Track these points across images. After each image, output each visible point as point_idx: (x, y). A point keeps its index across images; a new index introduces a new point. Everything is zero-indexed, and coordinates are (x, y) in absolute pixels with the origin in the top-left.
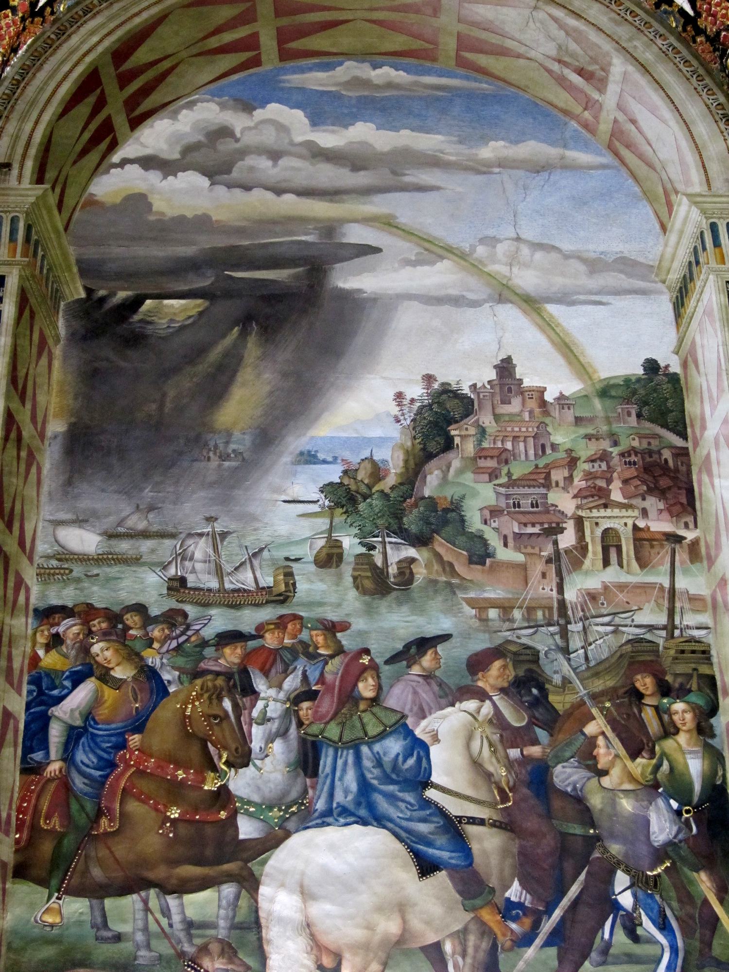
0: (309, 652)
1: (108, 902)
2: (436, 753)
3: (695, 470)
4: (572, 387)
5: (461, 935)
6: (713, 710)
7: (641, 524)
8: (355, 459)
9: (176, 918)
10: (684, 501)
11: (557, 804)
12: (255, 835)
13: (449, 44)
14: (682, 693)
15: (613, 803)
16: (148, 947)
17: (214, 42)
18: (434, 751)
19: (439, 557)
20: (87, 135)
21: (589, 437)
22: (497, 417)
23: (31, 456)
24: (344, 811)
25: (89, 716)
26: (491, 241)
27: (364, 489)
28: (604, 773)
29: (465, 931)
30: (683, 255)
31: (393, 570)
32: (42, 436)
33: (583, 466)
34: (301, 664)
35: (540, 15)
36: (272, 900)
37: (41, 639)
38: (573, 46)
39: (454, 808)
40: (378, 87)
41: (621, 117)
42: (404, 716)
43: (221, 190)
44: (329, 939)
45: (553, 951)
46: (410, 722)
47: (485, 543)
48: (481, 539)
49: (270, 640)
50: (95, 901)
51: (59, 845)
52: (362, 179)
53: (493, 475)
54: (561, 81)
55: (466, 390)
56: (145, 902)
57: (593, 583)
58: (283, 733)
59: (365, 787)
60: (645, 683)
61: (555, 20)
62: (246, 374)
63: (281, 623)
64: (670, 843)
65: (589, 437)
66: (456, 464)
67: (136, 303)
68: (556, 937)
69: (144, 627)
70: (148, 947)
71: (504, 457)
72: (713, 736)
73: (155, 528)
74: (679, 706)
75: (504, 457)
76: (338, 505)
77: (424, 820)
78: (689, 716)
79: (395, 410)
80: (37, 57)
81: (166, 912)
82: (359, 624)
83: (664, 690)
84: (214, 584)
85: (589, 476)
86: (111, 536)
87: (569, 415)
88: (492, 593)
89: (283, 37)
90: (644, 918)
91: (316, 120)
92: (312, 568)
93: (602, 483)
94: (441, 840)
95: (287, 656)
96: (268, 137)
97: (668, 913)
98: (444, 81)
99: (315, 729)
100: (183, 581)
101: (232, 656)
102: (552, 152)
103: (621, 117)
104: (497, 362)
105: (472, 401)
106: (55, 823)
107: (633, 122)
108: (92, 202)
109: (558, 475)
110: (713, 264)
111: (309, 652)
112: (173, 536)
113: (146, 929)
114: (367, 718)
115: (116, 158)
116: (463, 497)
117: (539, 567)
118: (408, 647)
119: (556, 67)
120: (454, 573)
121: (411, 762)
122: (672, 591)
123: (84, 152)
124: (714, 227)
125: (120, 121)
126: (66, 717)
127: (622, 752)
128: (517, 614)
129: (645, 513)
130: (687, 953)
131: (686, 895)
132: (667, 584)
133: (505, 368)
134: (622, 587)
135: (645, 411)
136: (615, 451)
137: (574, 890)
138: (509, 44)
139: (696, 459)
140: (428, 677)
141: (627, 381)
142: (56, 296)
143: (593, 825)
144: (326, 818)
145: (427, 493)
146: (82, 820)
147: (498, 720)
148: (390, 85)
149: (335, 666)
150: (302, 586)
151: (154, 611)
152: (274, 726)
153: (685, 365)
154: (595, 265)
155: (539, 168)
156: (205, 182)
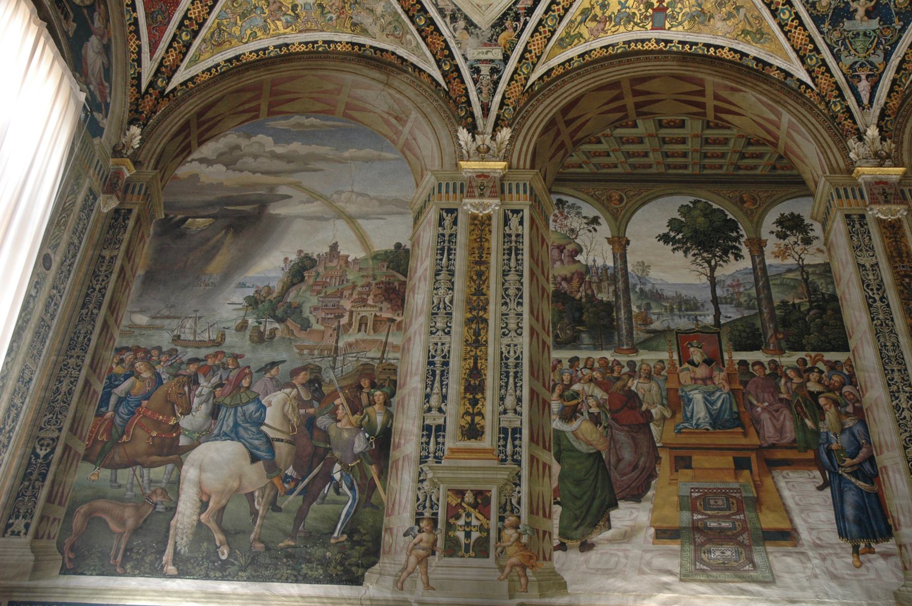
0: (224, 367)
1: (119, 471)
2: (269, 411)
3: (407, 291)
4: (361, 255)
5: (263, 489)
6: (393, 394)
7: (378, 314)
8: (261, 285)
9: (146, 478)
10: (399, 304)
11: (316, 433)
12: (186, 444)
13: (341, 108)
14: (381, 387)
15: (341, 434)
16: (132, 490)
17: (241, 108)
18: (268, 409)
19: (288, 327)
20: (179, 149)
21: (363, 276)
22: (326, 268)
23: (128, 284)
24: (226, 434)
25: (128, 393)
26: (339, 193)
27: (262, 299)
28: (339, 421)
29: (265, 487)
30: (424, 197)
31: (267, 333)
32: (134, 276)
33: (359, 289)
34: (220, 372)
35: (385, 93)
36: (187, 472)
37: (115, 361)
38: (396, 106)
39: (272, 434)
40: (307, 127)
41: (410, 138)
42: (259, 395)
43: (230, 172)
44: (207, 489)
45: (301, 497)
46: (260, 397)
47: (309, 322)
48: (307, 319)
49: (210, 362)
50: (114, 471)
51: (103, 447)
52: (292, 166)
53: (319, 292)
54: (387, 122)
55: (315, 257)
56: (134, 471)
57: (351, 339)
58: (206, 401)
59: (236, 425)
60: (365, 383)
61: (390, 95)
62: (224, 250)
63: (216, 355)
64: (362, 452)
65: (363, 276)
66: (304, 288)
67: (184, 220)
68: (304, 492)
69: (159, 356)
70: (132, 490)
71: (325, 285)
72: (390, 406)
73: (172, 315)
74: (378, 393)
75: (325, 285)
76: (250, 305)
77: (257, 439)
78: (381, 397)
79: (283, 265)
80: (165, 115)
81: (142, 476)
82: (248, 355)
83: (373, 385)
84: (192, 338)
85: (360, 293)
86: (154, 318)
87: (357, 267)
88: (309, 343)
89: (271, 105)
90: (344, 484)
91: (276, 142)
92: (234, 332)
93: (365, 296)
94: (263, 448)
95: (215, 368)
96: (255, 149)
97: (355, 483)
98: (335, 123)
99: (220, 400)
100: (179, 336)
101: (192, 368)
102: (376, 153)
103: (410, 138)
104: (331, 244)
105: (316, 261)
106: (105, 438)
107: (415, 139)
108: (176, 177)
109: (346, 293)
110: (436, 201)
111: (224, 367)
112: (179, 318)
113: (132, 483)
114: (243, 395)
115: (189, 159)
116: (303, 302)
117: (330, 331)
118: (266, 365)
119: (386, 116)
120: (293, 334)
121: (258, 414)
122: (386, 343)
123: (177, 156)
124: (440, 185)
125: (194, 143)
126: (119, 394)
127: (349, 412)
128: (316, 352)
129: (381, 309)
130: (359, 500)
131: (364, 475)
132: (384, 340)
133: (334, 247)
134: (364, 341)
135: (391, 266)
136: (374, 282)
137: (316, 471)
138: (367, 106)
139: (409, 286)
140: (272, 379)
141: (386, 252)
142: (153, 217)
143: (329, 443)
144: (218, 437)
145: (289, 300)
146: (115, 436)
147: (298, 397)
148: (312, 126)
149: (234, 373)
150: (228, 340)
151: (165, 349)
152: (203, 398)
153: (413, 246)
154: (382, 202)
155: (368, 160)
156: (224, 168)
